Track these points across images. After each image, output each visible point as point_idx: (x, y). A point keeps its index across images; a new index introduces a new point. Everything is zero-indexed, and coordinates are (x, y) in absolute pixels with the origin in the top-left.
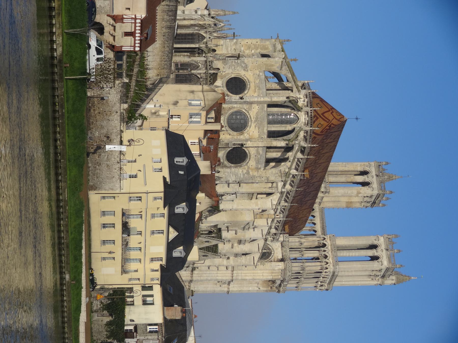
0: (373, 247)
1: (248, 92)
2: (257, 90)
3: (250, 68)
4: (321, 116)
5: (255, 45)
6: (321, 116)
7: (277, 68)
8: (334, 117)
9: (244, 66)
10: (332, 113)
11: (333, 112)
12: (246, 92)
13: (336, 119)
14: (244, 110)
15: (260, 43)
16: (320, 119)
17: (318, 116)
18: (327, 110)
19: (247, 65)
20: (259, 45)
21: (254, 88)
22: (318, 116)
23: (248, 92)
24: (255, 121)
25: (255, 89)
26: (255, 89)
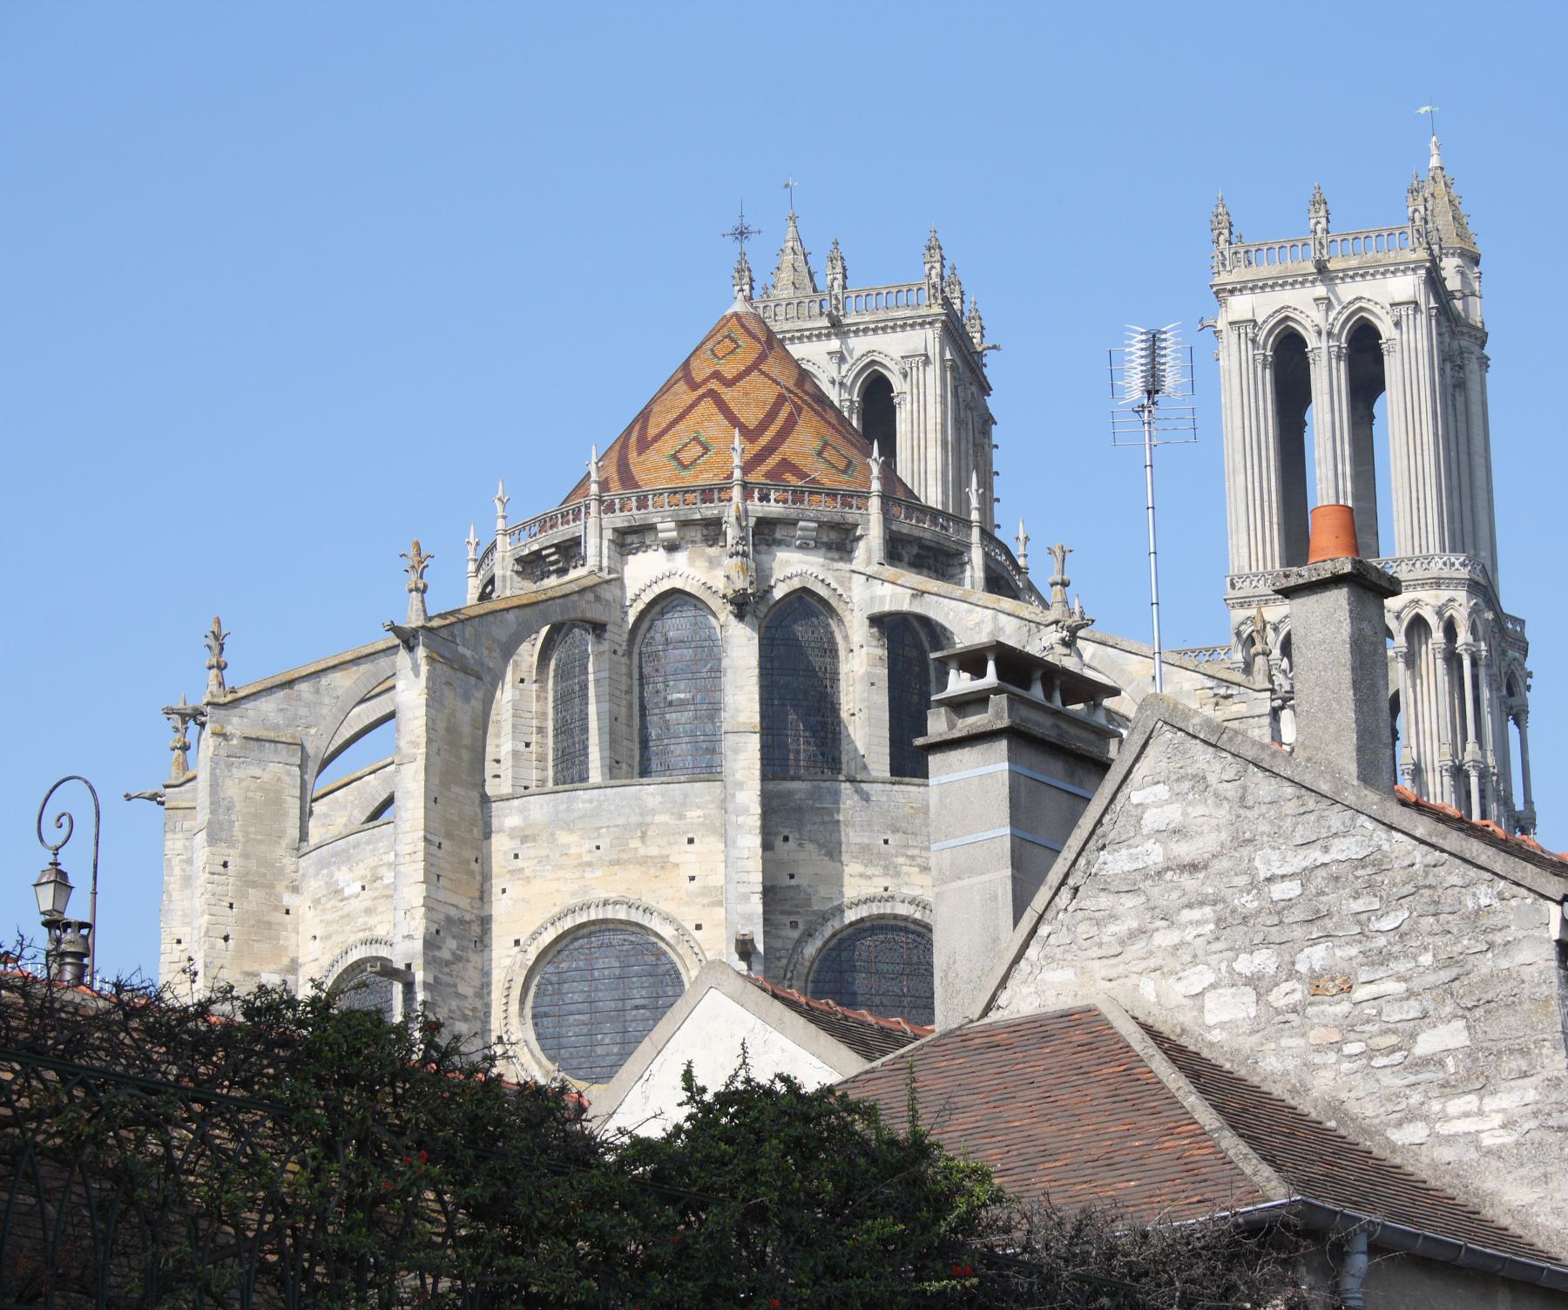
0: (1288, 357)
1: (667, 919)
2: (654, 851)
3: (464, 903)
4: (764, 440)
5: (247, 881)
6: (764, 440)
7: (467, 698)
8: (754, 366)
9: (452, 944)
10: (729, 383)
11: (717, 375)
12: (667, 931)
13: (762, 358)
14: (810, 950)
15: (231, 842)
16: (787, 449)
17: (772, 461)
18: (707, 406)
19: (449, 919)
20: (245, 856)
21: (635, 872)
22: (772, 461)
23: (667, 919)
24: (891, 870)
25: (644, 861)
26: (644, 861)
